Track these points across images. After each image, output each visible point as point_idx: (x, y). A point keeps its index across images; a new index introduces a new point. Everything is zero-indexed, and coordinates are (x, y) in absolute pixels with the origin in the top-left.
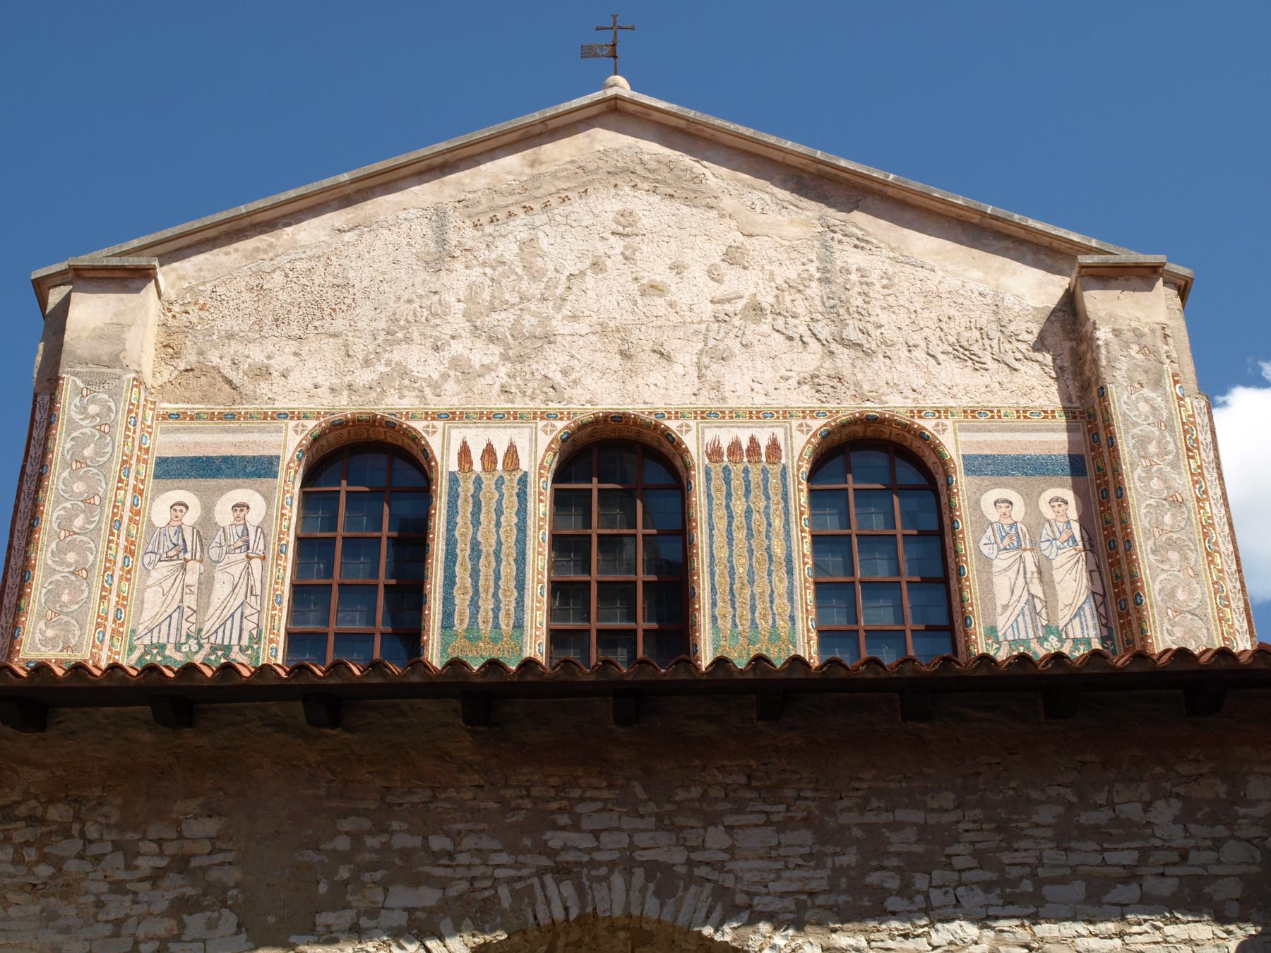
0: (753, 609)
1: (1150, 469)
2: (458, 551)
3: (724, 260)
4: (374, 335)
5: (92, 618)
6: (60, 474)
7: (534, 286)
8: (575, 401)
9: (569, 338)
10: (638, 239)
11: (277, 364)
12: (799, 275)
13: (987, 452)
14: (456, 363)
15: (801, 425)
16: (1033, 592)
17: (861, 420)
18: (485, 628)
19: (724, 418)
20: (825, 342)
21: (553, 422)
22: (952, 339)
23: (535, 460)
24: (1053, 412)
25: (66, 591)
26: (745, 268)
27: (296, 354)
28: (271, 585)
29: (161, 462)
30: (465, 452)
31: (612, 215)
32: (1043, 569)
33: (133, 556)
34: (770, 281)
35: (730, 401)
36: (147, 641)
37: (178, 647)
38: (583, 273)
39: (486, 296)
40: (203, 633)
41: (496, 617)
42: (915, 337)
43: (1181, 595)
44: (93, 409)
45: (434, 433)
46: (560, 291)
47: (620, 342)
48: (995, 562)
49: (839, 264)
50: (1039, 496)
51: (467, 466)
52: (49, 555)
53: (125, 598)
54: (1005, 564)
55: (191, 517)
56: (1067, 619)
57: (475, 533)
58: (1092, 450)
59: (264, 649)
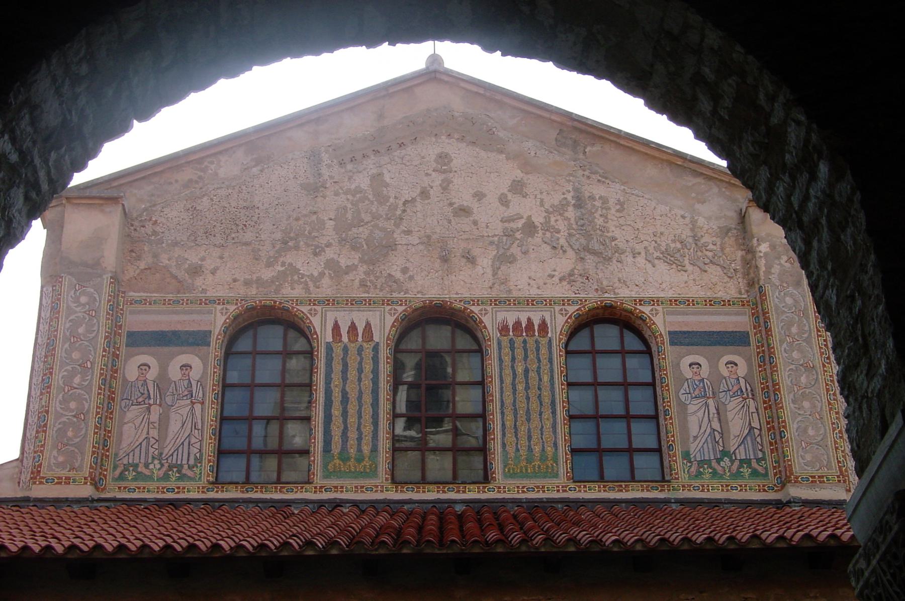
0: (530, 438)
1: (792, 345)
2: (333, 398)
3: (509, 191)
4: (272, 244)
5: (89, 449)
6: (63, 346)
7: (380, 209)
8: (410, 292)
9: (405, 247)
10: (451, 175)
11: (209, 264)
12: (560, 201)
13: (685, 329)
14: (331, 264)
15: (561, 310)
16: (714, 427)
17: (602, 306)
18: (352, 451)
19: (510, 304)
20: (577, 251)
21: (395, 307)
22: (663, 249)
23: (384, 335)
24: (729, 301)
25: (71, 429)
26: (523, 197)
27: (221, 258)
28: (208, 422)
29: (130, 334)
30: (336, 328)
31: (433, 157)
32: (720, 411)
33: (114, 402)
34: (541, 206)
35: (514, 292)
36: (125, 462)
37: (146, 466)
38: (413, 200)
39: (349, 216)
40: (163, 456)
41: (359, 444)
42: (637, 247)
43: (811, 432)
44: (83, 299)
45: (316, 314)
46: (399, 212)
47: (439, 250)
48: (689, 407)
49: (587, 194)
50: (719, 360)
51: (338, 338)
52: (58, 404)
53: (110, 432)
54: (695, 408)
55: (152, 375)
56: (736, 446)
57: (344, 385)
58: (754, 329)
59: (205, 466)
